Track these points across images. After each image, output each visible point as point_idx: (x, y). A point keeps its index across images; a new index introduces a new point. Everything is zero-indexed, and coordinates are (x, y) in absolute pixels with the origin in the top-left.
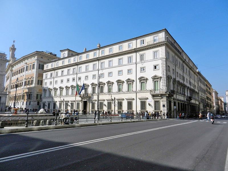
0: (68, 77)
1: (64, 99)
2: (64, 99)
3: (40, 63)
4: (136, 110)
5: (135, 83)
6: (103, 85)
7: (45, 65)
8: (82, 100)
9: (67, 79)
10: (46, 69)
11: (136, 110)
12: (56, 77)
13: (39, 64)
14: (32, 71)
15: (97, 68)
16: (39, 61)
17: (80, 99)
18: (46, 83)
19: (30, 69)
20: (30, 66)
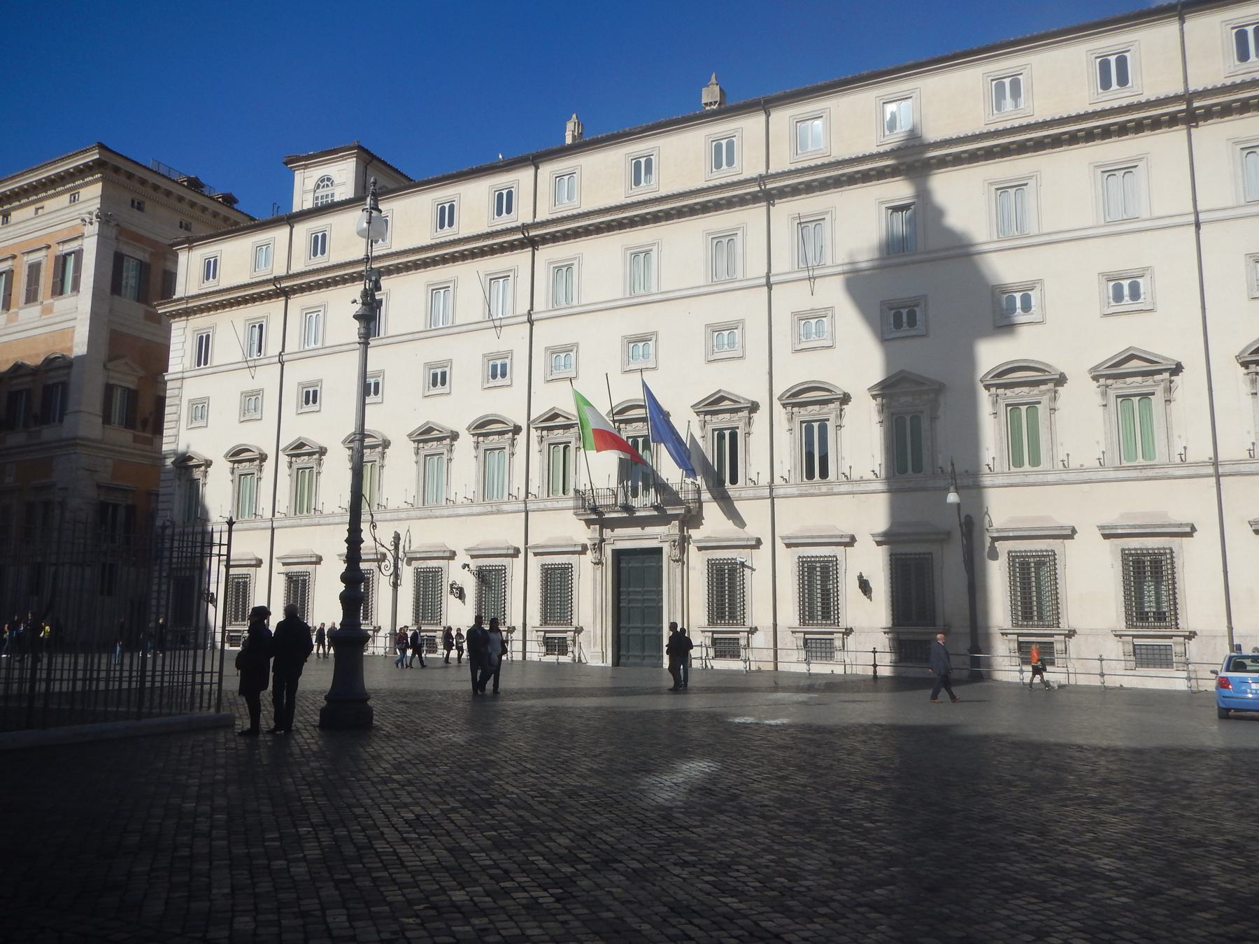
0: (436, 351)
1: (397, 538)
2: (397, 538)
3: (126, 250)
4: (1230, 629)
5: (1189, 386)
6: (738, 420)
7: (183, 257)
8: (599, 546)
9: (479, 360)
10: (193, 291)
11: (1230, 629)
12: (303, 355)
13: (119, 258)
14: (47, 310)
15: (758, 269)
16: (112, 232)
17: (583, 534)
18: (200, 410)
19: (31, 297)
20: (34, 269)
